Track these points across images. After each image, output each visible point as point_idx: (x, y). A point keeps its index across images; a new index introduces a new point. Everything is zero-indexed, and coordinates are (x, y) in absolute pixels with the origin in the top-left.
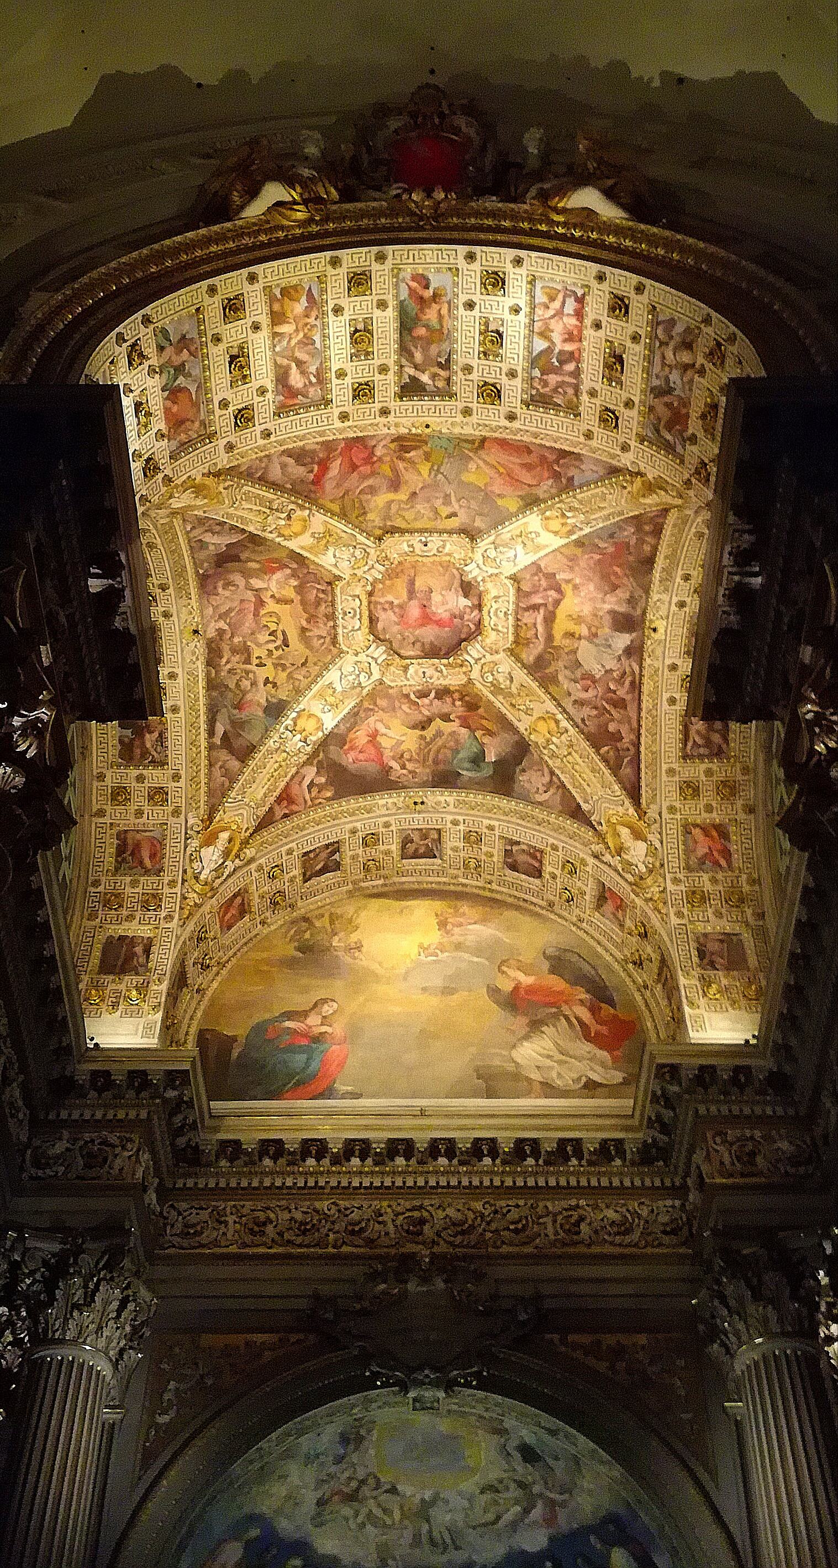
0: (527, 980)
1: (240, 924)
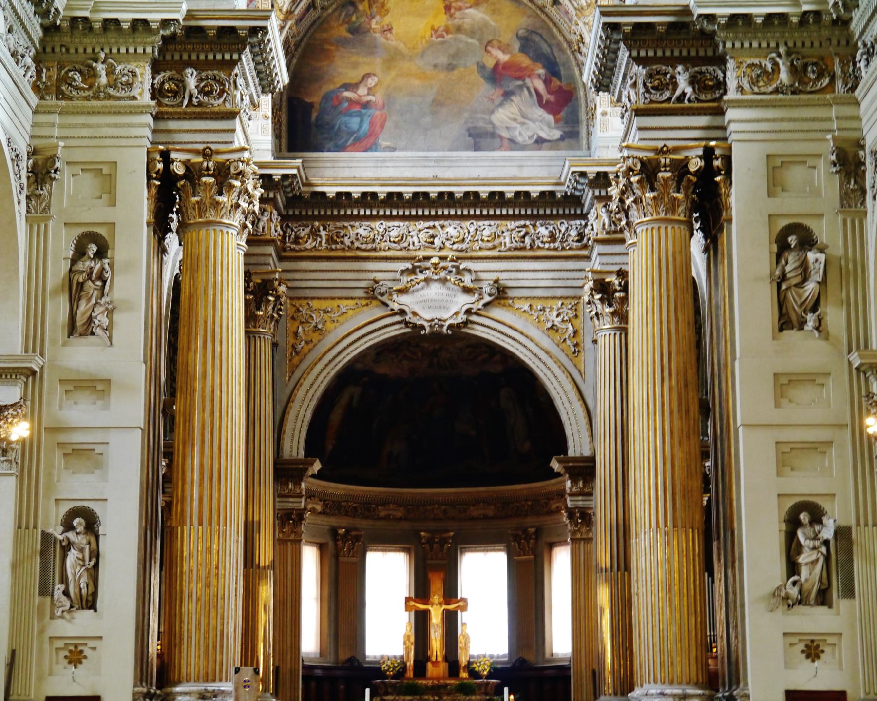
0: (504, 58)
1: (309, 14)
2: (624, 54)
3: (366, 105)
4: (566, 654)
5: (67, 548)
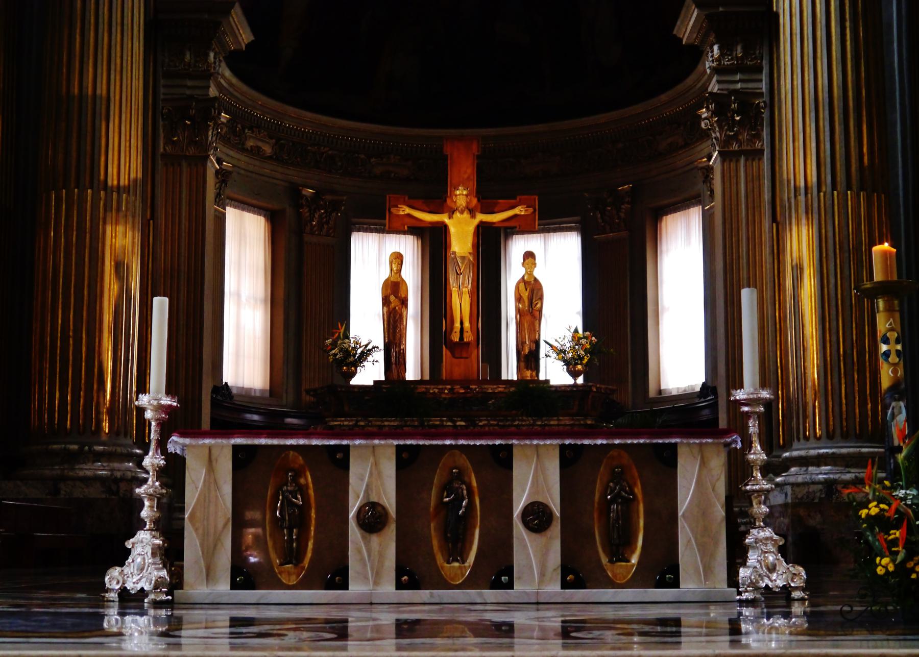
4: (692, 387)
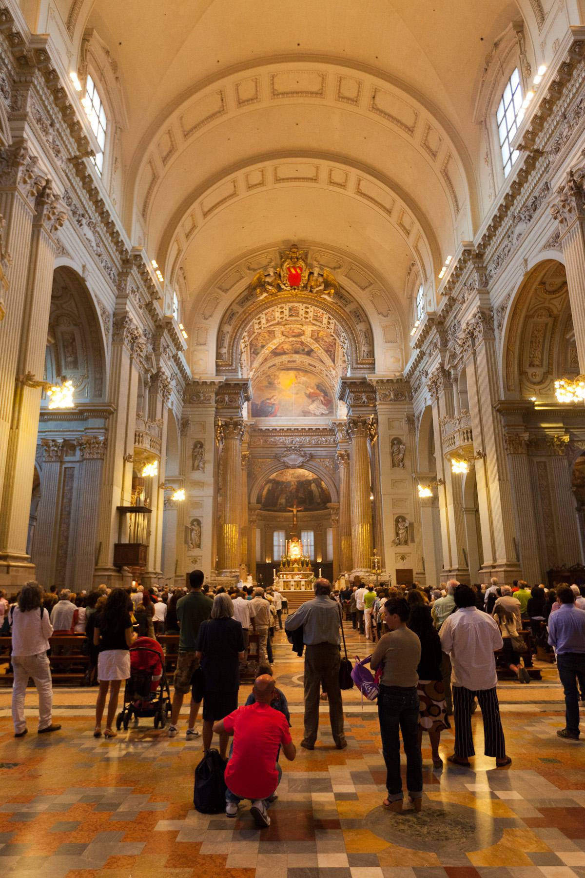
0: (312, 391)
2: (348, 391)
3: (274, 404)
5: (192, 530)
